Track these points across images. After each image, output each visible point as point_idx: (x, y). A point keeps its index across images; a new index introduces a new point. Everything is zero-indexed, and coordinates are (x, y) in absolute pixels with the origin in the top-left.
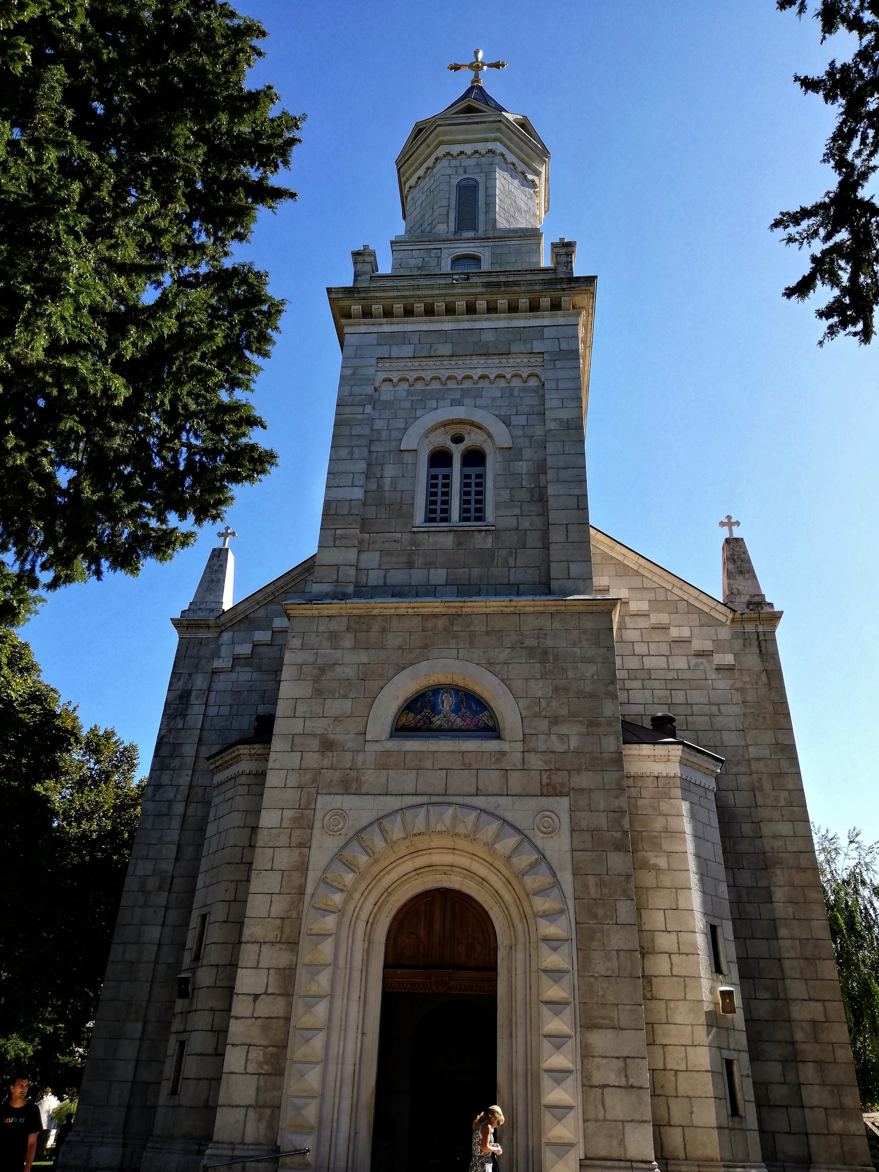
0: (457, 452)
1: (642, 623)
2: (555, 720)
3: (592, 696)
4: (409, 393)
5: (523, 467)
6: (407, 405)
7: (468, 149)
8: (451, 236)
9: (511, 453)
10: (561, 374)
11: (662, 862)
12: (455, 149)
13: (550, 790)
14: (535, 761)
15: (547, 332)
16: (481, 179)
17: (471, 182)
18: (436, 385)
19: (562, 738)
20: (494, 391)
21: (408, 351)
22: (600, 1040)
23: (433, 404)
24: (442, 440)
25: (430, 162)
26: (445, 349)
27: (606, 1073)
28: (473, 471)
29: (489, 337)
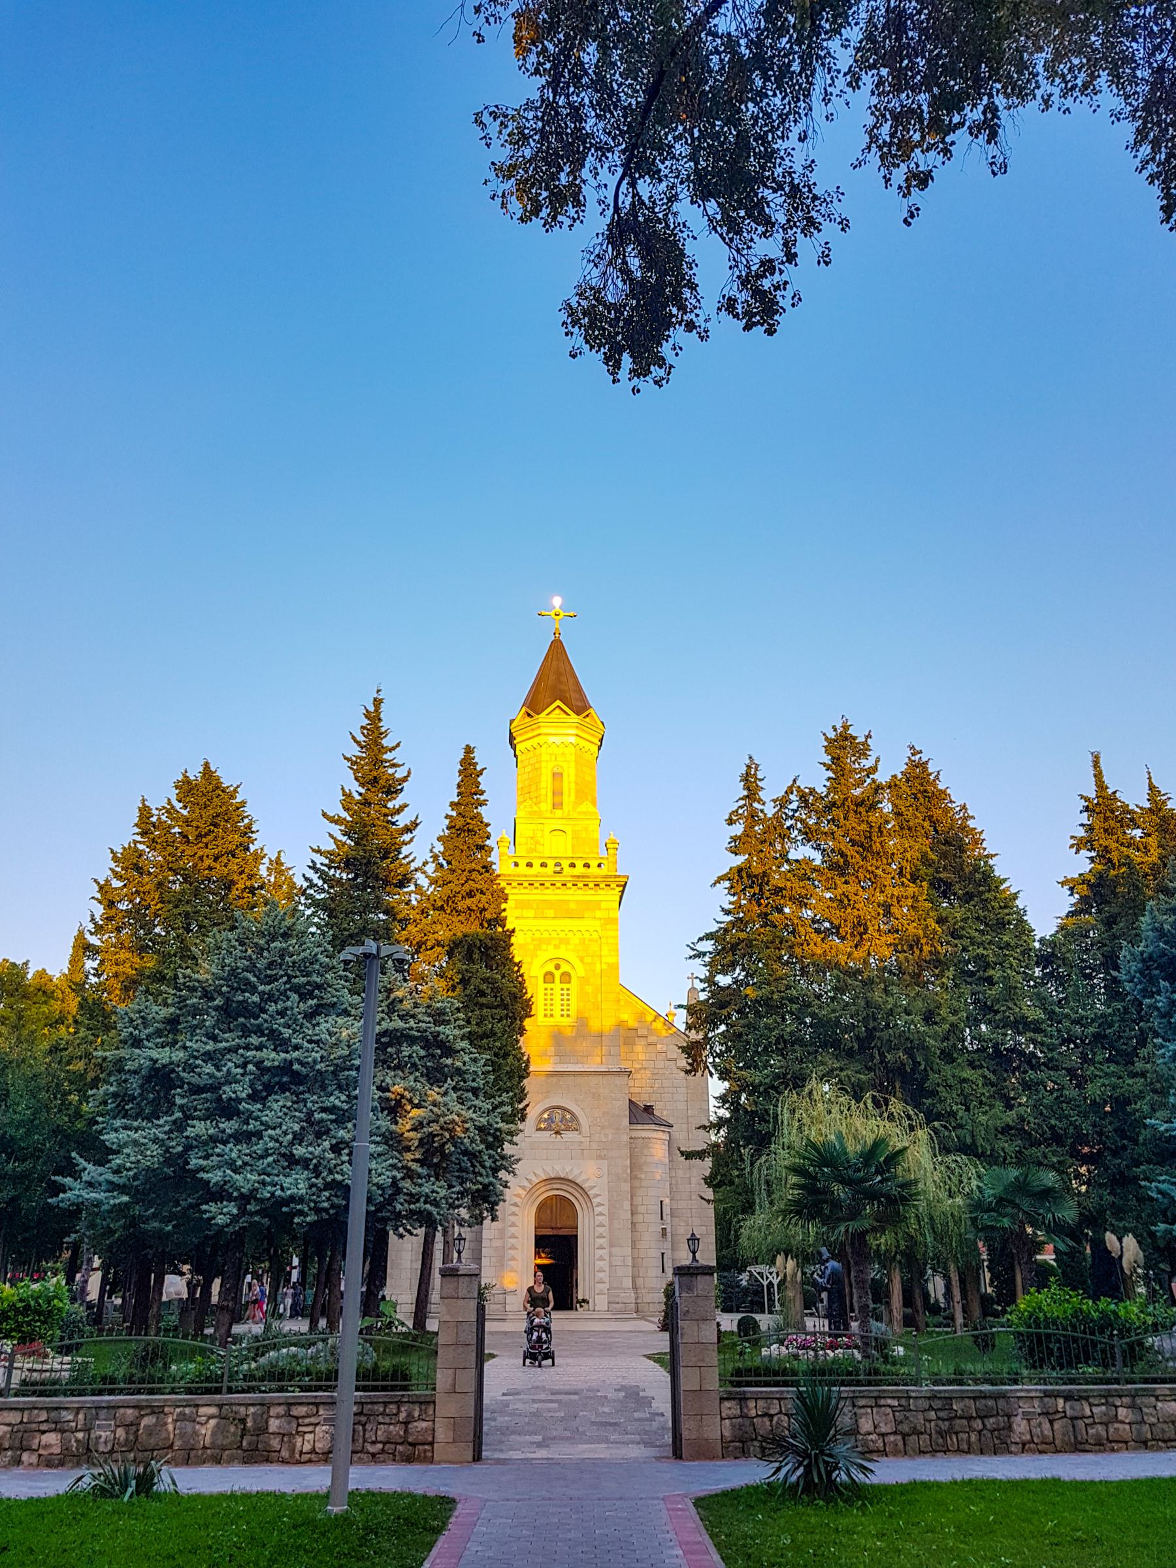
0: (557, 974)
1: (643, 1042)
2: (603, 1128)
3: (619, 1116)
4: (533, 940)
5: (589, 989)
6: (532, 947)
7: (558, 740)
8: (549, 815)
9: (584, 981)
10: (610, 933)
11: (643, 1176)
12: (551, 739)
13: (600, 1157)
14: (594, 1146)
15: (603, 905)
16: (565, 765)
17: (560, 770)
18: (546, 935)
19: (606, 1135)
20: (575, 940)
21: (531, 913)
22: (615, 1250)
23: (544, 947)
24: (550, 967)
25: (534, 742)
26: (551, 913)
27: (617, 1261)
28: (565, 986)
29: (573, 906)
